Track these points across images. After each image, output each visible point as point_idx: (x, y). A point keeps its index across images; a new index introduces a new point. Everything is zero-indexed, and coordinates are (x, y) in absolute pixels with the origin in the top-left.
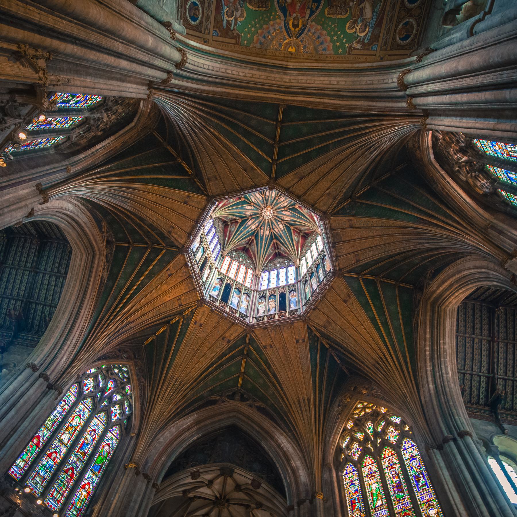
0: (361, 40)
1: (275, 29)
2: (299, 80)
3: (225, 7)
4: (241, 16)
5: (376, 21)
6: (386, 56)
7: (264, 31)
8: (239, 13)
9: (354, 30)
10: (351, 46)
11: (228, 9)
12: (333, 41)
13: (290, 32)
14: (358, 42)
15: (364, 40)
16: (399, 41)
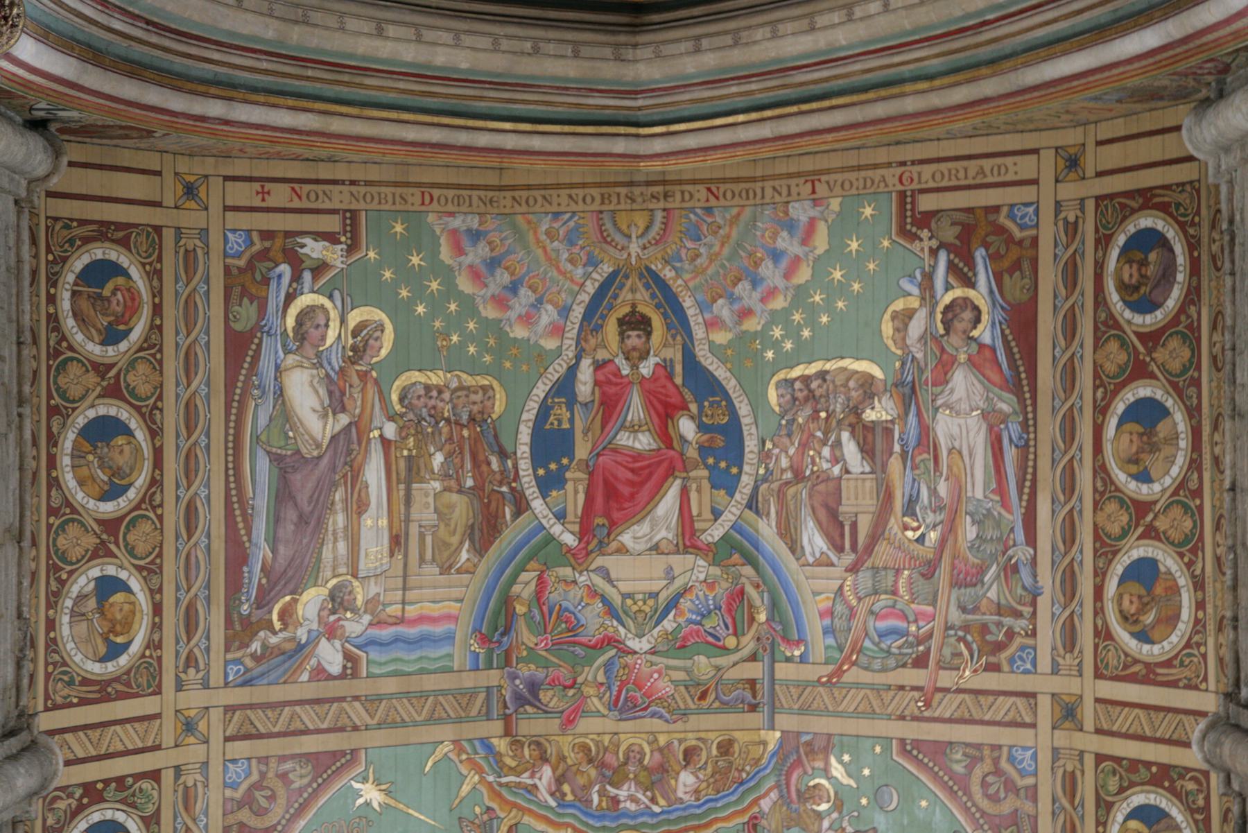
0: (307, 276)
1: (732, 299)
2: (576, 55)
3: (987, 339)
4: (905, 318)
5: (256, 358)
6: (169, 200)
7: (780, 282)
8: (916, 327)
9: (352, 324)
10: (352, 248)
11: (975, 333)
12: (447, 275)
13: (653, 296)
14: (320, 268)
15: (296, 277)
16: (124, 261)
